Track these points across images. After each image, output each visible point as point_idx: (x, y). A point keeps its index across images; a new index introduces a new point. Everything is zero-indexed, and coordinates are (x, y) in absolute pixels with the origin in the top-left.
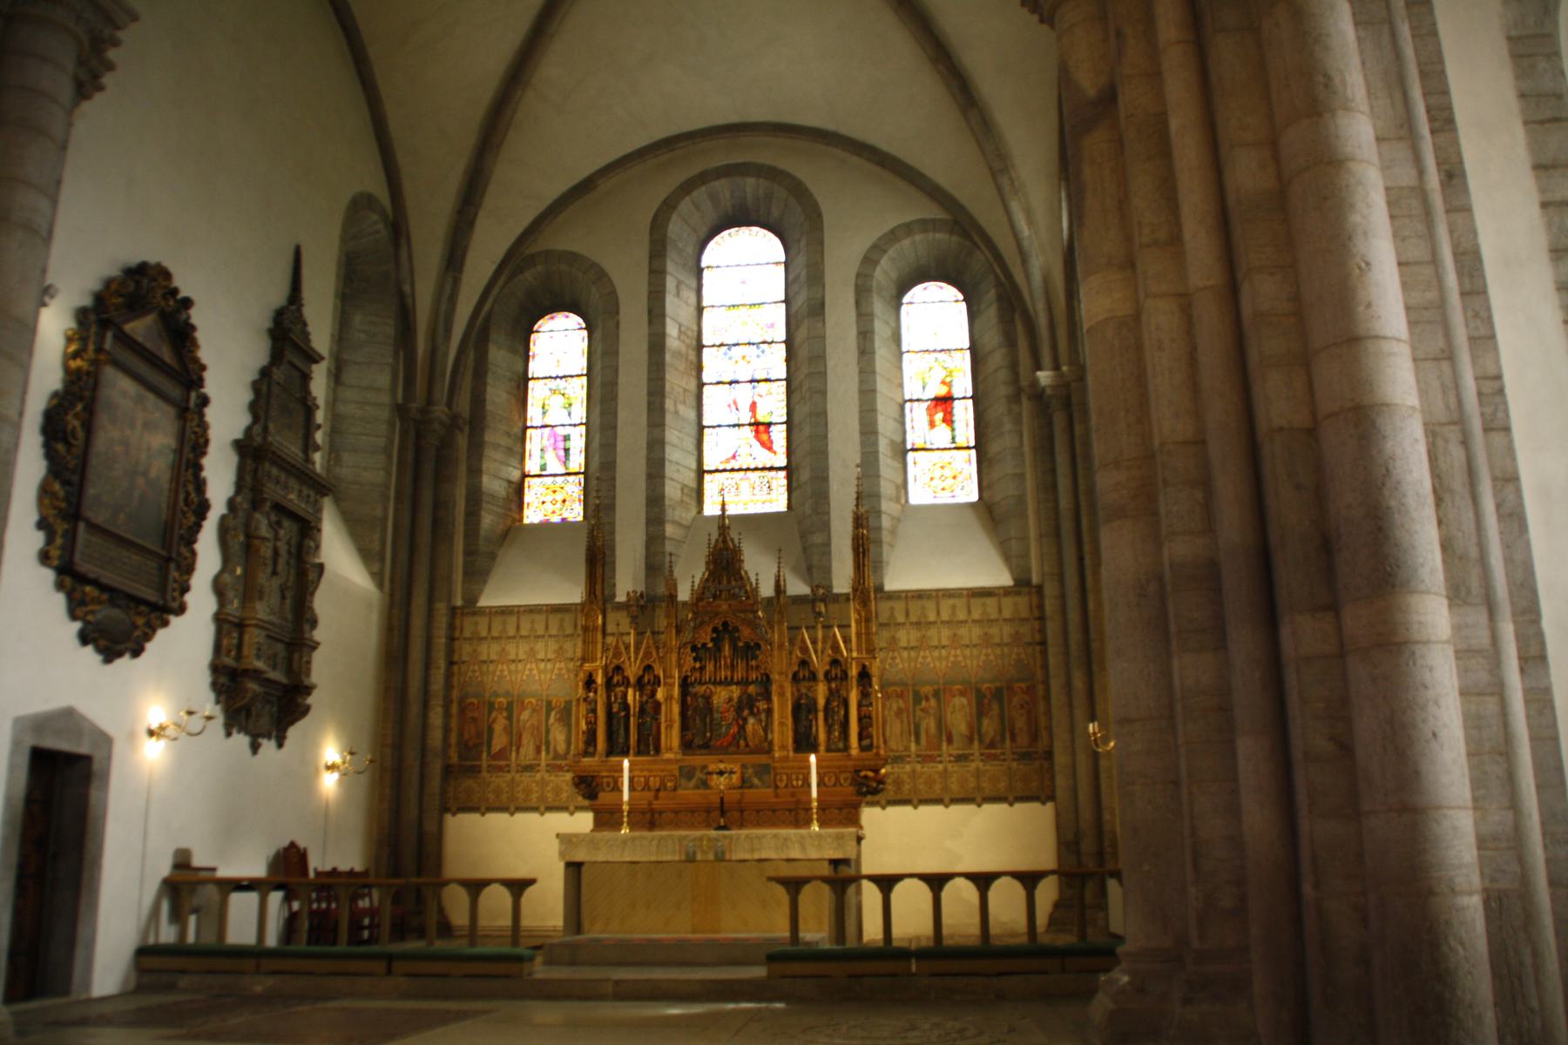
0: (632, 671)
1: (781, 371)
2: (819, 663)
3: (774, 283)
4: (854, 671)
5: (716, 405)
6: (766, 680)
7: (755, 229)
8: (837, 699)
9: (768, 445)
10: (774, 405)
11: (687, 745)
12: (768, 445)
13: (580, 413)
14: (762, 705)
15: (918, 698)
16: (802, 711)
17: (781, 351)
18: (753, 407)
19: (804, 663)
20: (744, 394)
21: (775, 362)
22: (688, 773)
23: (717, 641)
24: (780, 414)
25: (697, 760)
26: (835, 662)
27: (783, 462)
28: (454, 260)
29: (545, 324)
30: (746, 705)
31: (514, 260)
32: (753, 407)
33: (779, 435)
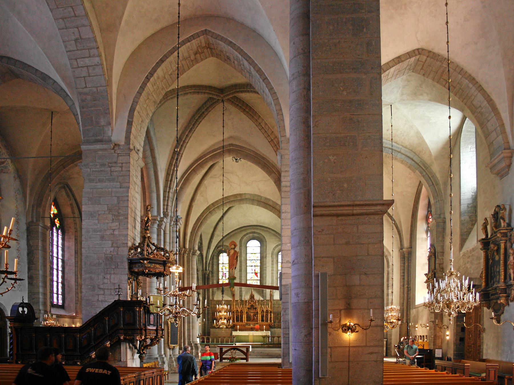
0: (239, 310)
1: (259, 265)
2: (265, 310)
3: (258, 250)
4: (269, 312)
5: (249, 269)
6: (257, 312)
7: (255, 241)
8: (267, 315)
9: (257, 276)
10: (258, 270)
11: (247, 320)
12: (257, 276)
13: (228, 270)
14: (257, 315)
15: (278, 314)
16: (262, 317)
17: (259, 261)
18: (255, 270)
19: (263, 310)
20: (253, 268)
21: (258, 263)
22: (247, 324)
23: (251, 307)
24: (259, 272)
25: (249, 322)
26: (267, 310)
27: (259, 279)
28: (209, 248)
29: (221, 255)
30: (254, 315)
31: (217, 247)
32: (255, 270)
33: (259, 275)
